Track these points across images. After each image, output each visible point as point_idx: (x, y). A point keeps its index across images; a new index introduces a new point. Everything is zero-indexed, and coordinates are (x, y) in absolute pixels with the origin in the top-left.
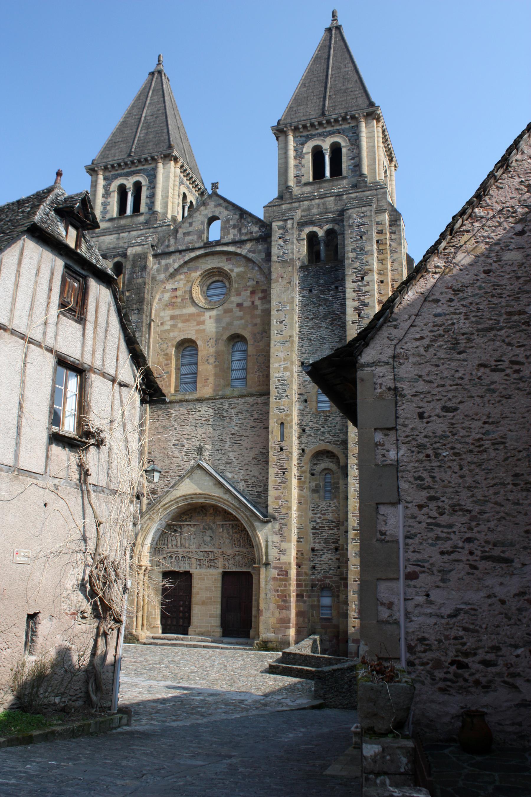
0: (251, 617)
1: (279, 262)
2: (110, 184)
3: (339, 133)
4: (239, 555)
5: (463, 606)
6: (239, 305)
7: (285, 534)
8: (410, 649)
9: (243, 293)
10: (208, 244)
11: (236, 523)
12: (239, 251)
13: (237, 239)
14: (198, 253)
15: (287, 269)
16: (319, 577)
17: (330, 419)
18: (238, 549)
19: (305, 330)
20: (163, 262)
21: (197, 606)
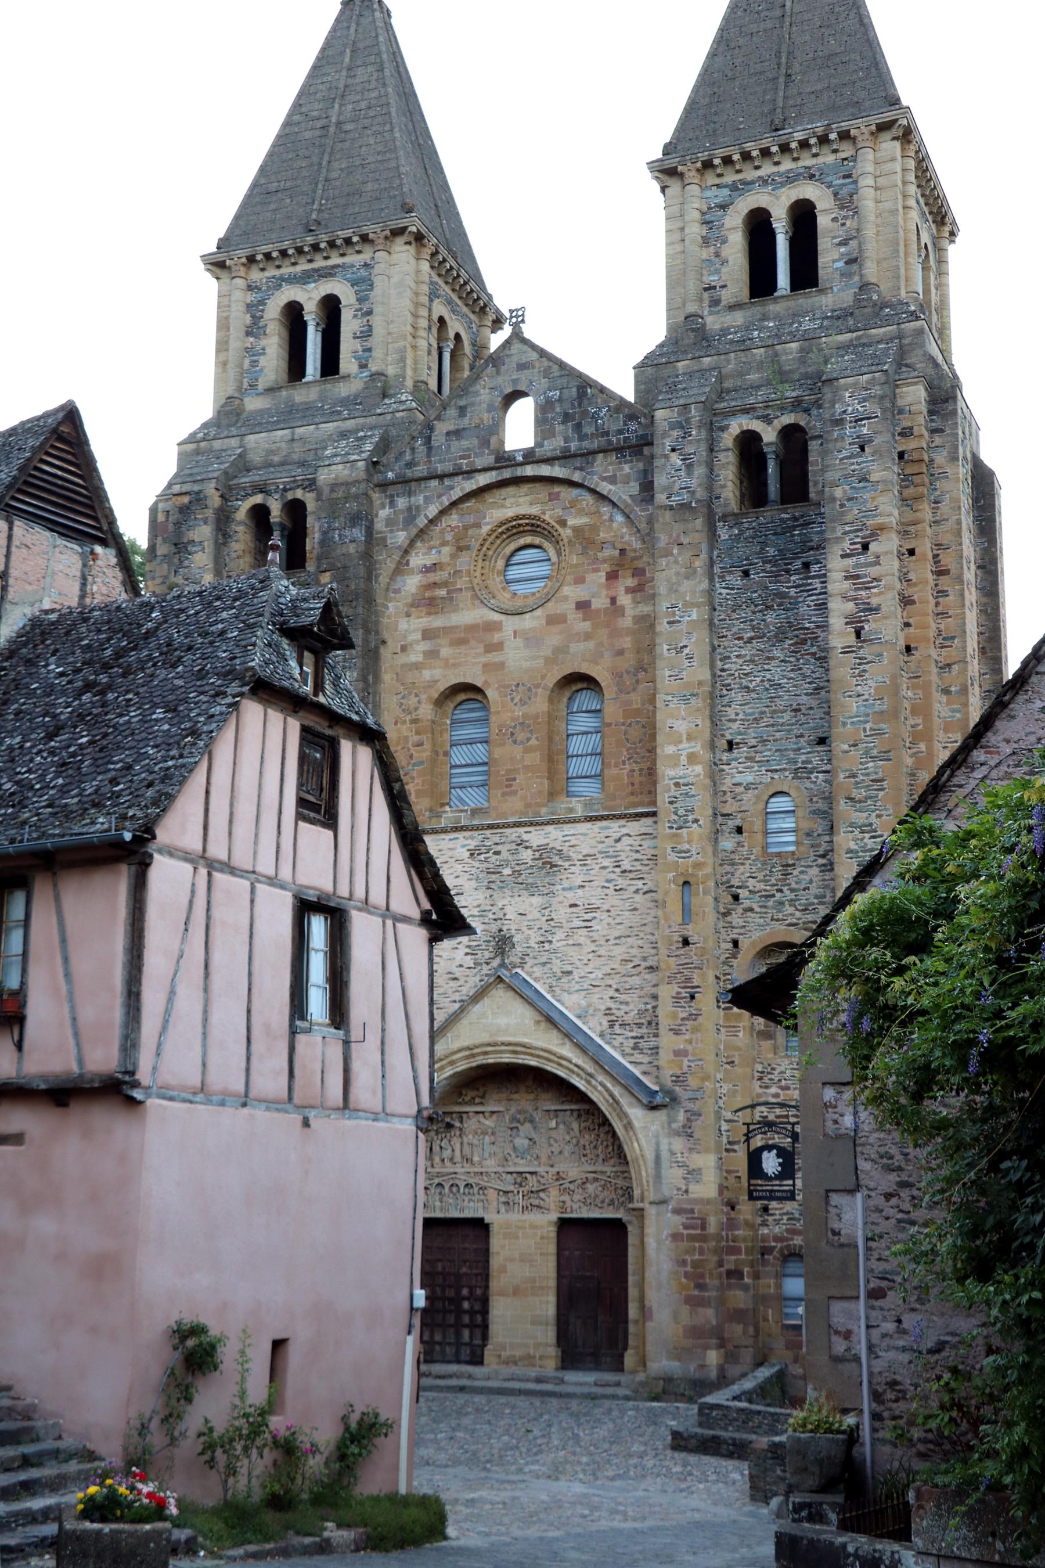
0: (626, 1321)
1: (671, 508)
2: (262, 302)
3: (812, 177)
4: (596, 1180)
5: (948, 1338)
6: (582, 606)
7: (696, 1135)
8: (876, 1396)
9: (590, 577)
10: (504, 460)
12: (577, 477)
13: (573, 446)
14: (483, 479)
15: (690, 526)
16: (777, 1230)
17: (795, 873)
18: (591, 1169)
19: (734, 667)
20: (401, 503)
21: (502, 1299)
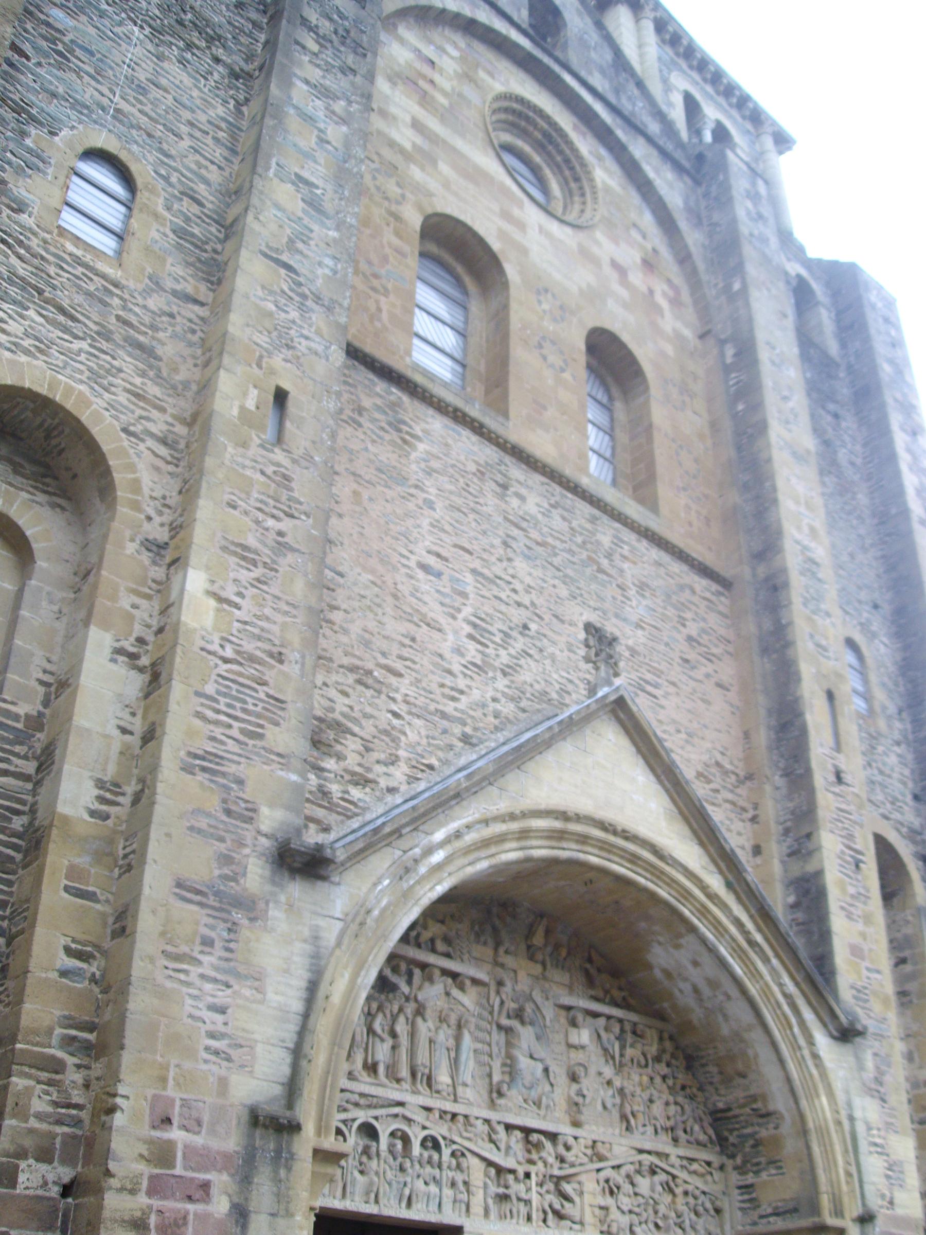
11: (633, 1017)
